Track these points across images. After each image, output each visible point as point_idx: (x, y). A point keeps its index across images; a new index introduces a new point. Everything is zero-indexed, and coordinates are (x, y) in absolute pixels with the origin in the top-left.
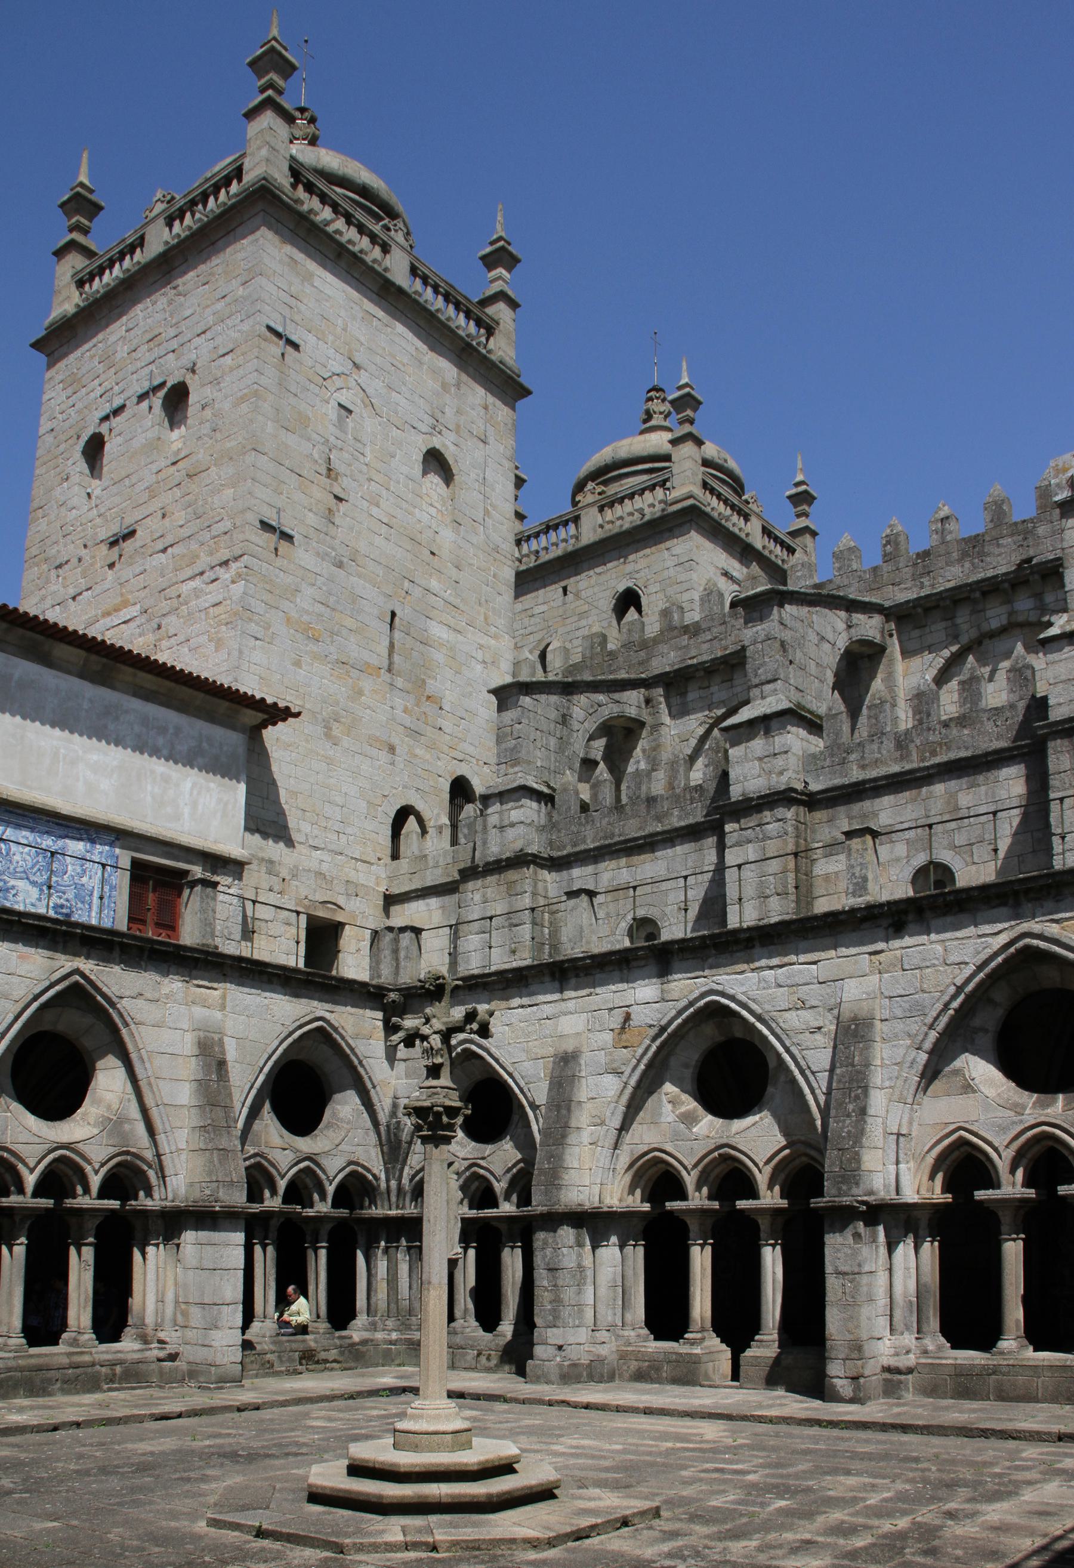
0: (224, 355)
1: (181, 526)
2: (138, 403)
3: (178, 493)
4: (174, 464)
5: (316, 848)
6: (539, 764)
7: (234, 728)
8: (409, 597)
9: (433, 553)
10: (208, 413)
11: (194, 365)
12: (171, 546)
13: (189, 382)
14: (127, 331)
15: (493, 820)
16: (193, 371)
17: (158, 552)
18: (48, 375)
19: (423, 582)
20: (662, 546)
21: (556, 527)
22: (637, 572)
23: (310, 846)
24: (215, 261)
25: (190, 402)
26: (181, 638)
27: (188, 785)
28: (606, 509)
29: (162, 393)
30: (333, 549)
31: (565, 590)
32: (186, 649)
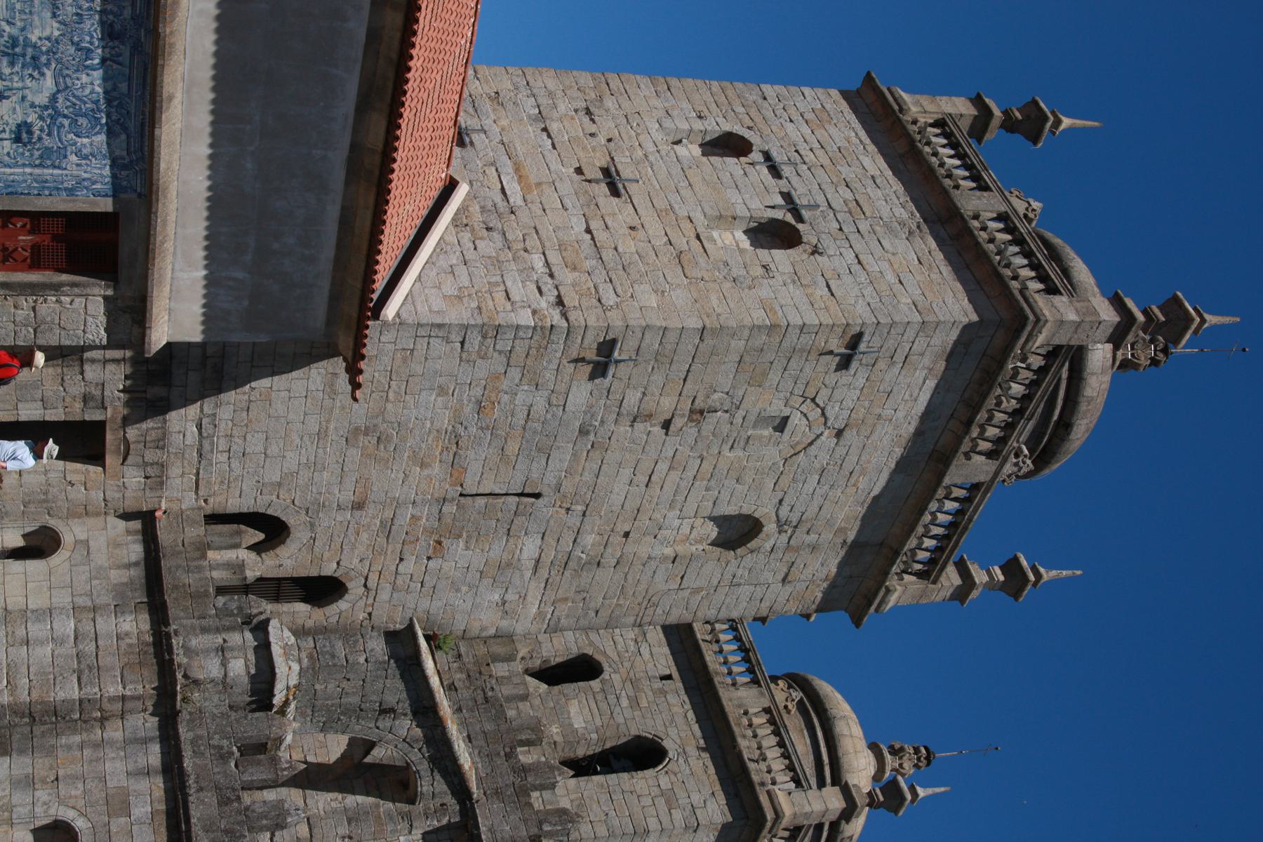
0: (828, 286)
1: (616, 249)
2: (781, 193)
3: (660, 241)
4: (698, 237)
5: (199, 426)
6: (318, 687)
7: (329, 323)
8: (563, 511)
9: (627, 535)
10: (759, 271)
11: (820, 254)
12: (593, 239)
13: (800, 248)
14: (873, 177)
15: (235, 638)
16: (813, 253)
17: (587, 222)
18: (835, 93)
19: (587, 527)
20: (718, 787)
21: (746, 660)
22: (686, 761)
23: (201, 420)
24: (946, 270)
25: (774, 252)
26: (470, 255)
27: (240, 275)
28: (768, 716)
29: (789, 218)
30: (602, 422)
31: (669, 677)
32: (454, 261)
